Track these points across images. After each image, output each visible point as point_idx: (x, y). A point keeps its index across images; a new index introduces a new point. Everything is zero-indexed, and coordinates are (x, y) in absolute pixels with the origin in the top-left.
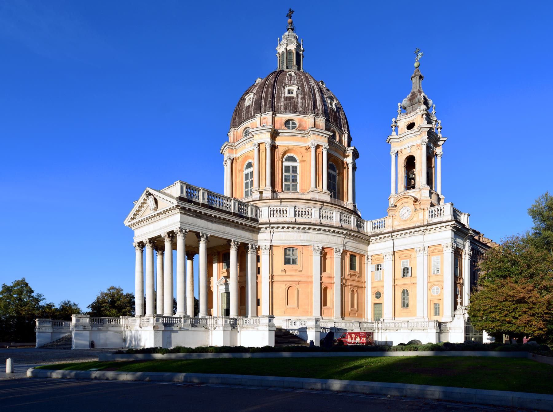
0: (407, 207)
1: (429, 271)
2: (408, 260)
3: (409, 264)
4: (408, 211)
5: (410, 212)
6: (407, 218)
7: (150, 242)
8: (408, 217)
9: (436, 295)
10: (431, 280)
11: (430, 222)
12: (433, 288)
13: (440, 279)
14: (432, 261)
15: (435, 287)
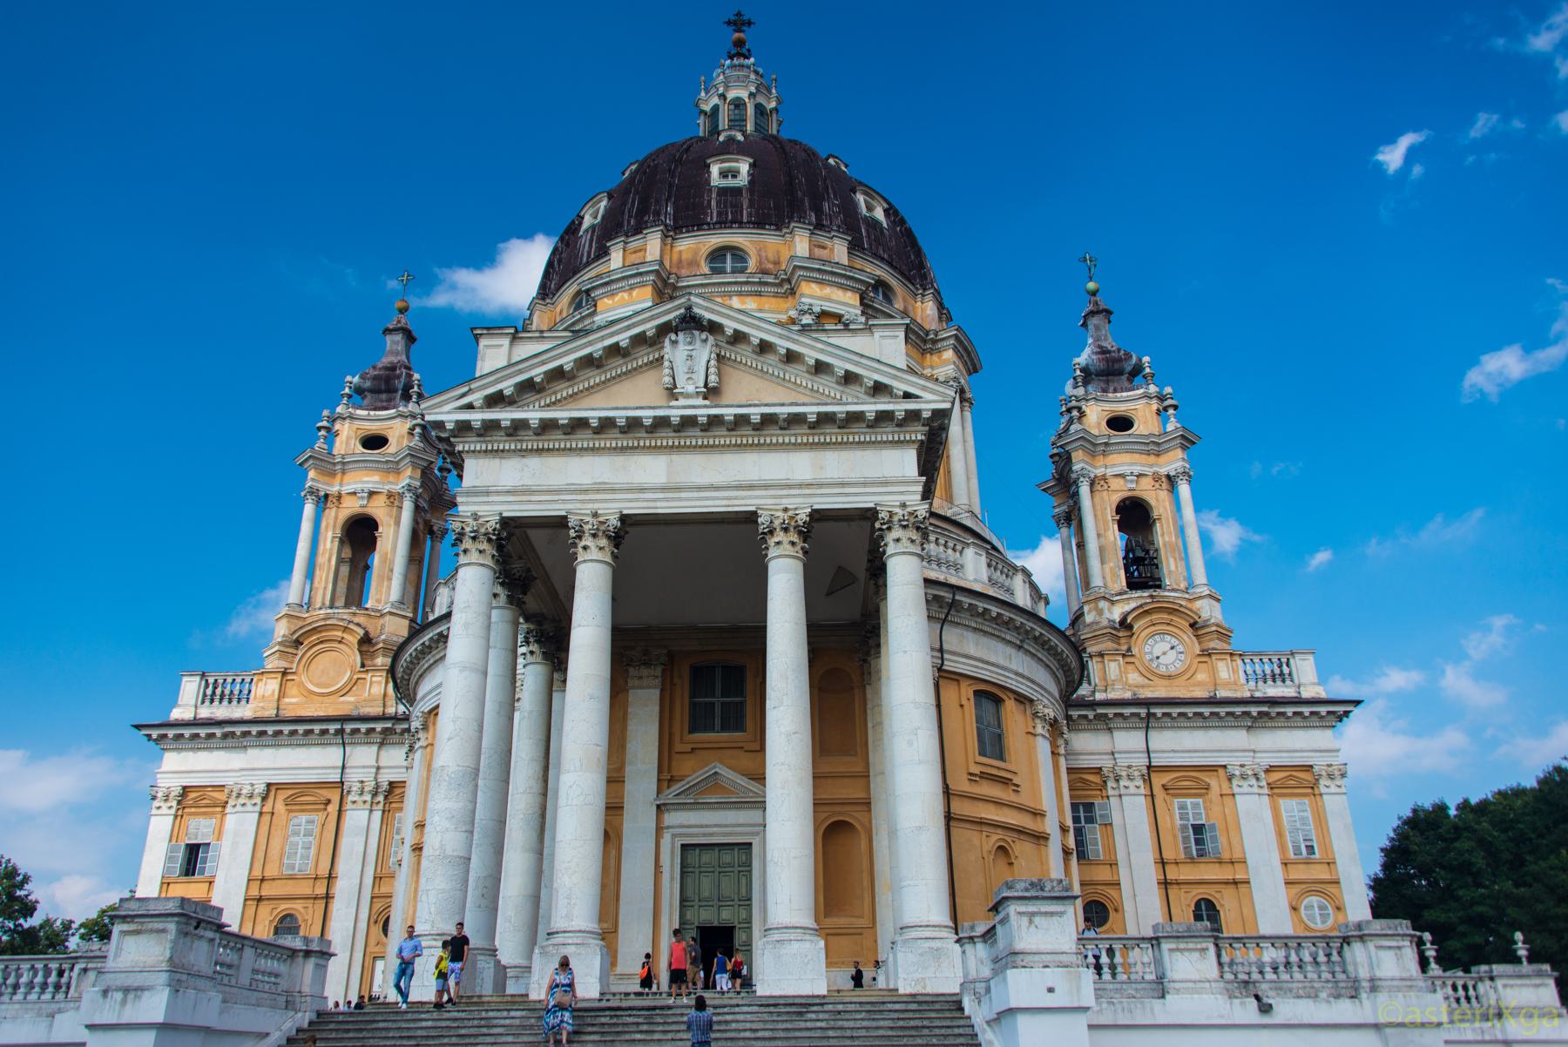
0: (1169, 637)
1: (1282, 847)
2: (1200, 800)
3: (1207, 815)
4: (1172, 648)
5: (1181, 653)
6: (1172, 670)
7: (617, 538)
8: (1178, 666)
9: (1320, 926)
10: (1293, 876)
11: (1257, 694)
12: (1307, 900)
13: (1325, 876)
14: (1284, 814)
15: (1314, 900)
